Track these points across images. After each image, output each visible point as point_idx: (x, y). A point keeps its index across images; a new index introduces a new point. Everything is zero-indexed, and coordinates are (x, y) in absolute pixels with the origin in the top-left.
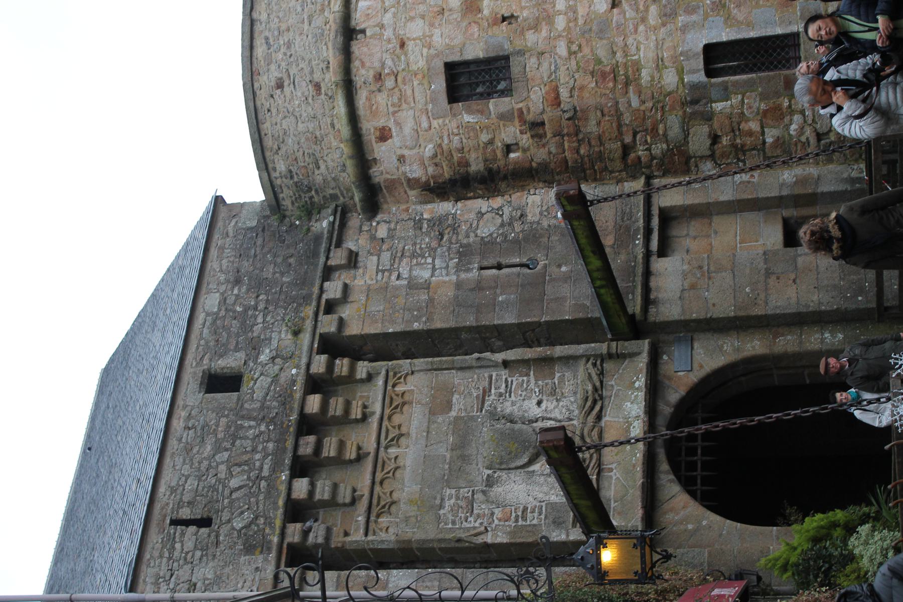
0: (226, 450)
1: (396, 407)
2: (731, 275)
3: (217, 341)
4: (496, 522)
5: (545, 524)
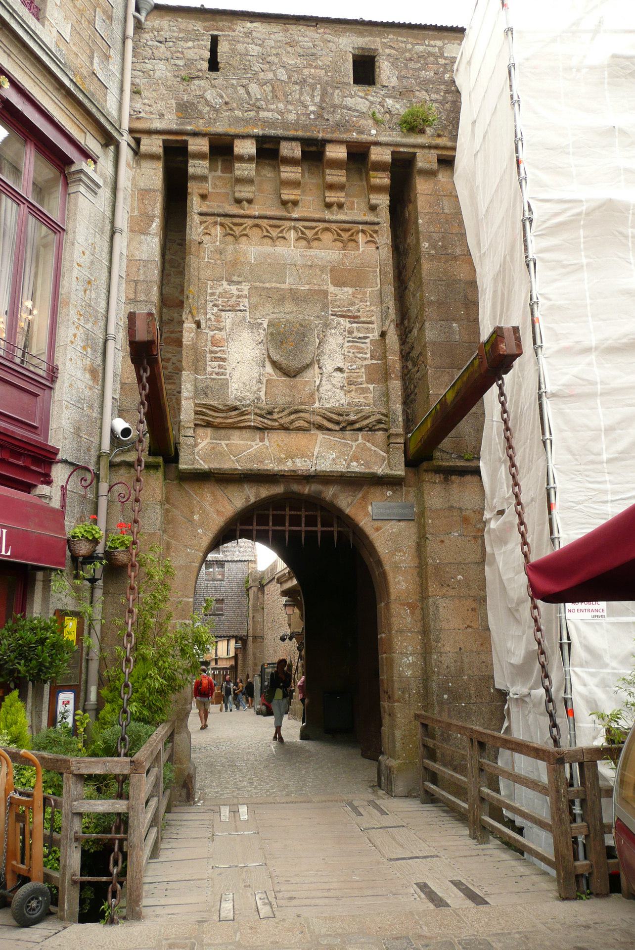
0: (289, 78)
1: (339, 235)
3: (411, 60)
4: (212, 333)
5: (207, 378)
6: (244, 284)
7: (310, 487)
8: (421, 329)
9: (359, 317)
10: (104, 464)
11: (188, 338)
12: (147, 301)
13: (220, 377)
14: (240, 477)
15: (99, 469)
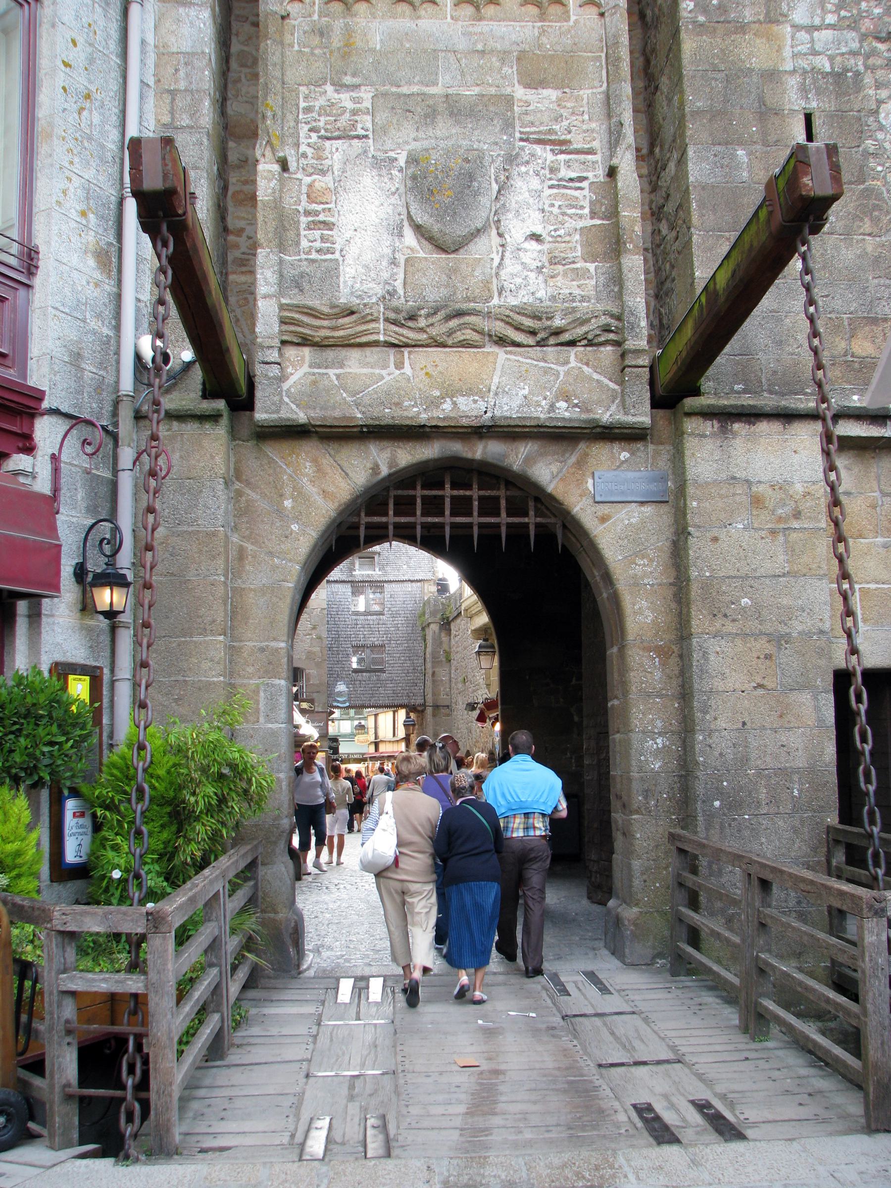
2: (777, 572)
4: (308, 180)
5: (300, 260)
6: (363, 88)
7: (485, 447)
8: (682, 161)
9: (570, 142)
10: (126, 414)
11: (266, 189)
12: (192, 127)
13: (324, 257)
14: (363, 432)
15: (116, 424)
